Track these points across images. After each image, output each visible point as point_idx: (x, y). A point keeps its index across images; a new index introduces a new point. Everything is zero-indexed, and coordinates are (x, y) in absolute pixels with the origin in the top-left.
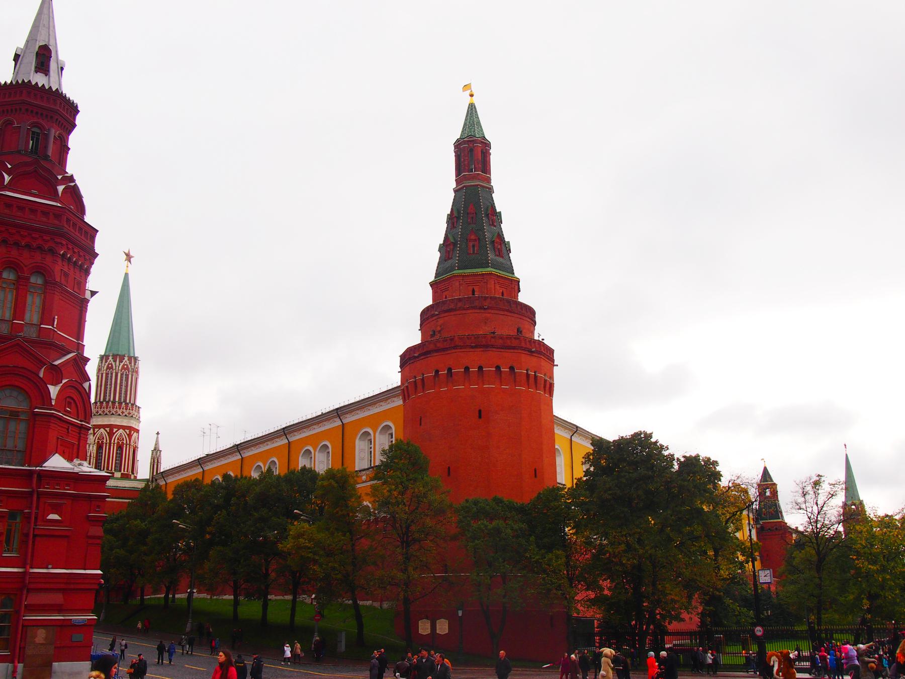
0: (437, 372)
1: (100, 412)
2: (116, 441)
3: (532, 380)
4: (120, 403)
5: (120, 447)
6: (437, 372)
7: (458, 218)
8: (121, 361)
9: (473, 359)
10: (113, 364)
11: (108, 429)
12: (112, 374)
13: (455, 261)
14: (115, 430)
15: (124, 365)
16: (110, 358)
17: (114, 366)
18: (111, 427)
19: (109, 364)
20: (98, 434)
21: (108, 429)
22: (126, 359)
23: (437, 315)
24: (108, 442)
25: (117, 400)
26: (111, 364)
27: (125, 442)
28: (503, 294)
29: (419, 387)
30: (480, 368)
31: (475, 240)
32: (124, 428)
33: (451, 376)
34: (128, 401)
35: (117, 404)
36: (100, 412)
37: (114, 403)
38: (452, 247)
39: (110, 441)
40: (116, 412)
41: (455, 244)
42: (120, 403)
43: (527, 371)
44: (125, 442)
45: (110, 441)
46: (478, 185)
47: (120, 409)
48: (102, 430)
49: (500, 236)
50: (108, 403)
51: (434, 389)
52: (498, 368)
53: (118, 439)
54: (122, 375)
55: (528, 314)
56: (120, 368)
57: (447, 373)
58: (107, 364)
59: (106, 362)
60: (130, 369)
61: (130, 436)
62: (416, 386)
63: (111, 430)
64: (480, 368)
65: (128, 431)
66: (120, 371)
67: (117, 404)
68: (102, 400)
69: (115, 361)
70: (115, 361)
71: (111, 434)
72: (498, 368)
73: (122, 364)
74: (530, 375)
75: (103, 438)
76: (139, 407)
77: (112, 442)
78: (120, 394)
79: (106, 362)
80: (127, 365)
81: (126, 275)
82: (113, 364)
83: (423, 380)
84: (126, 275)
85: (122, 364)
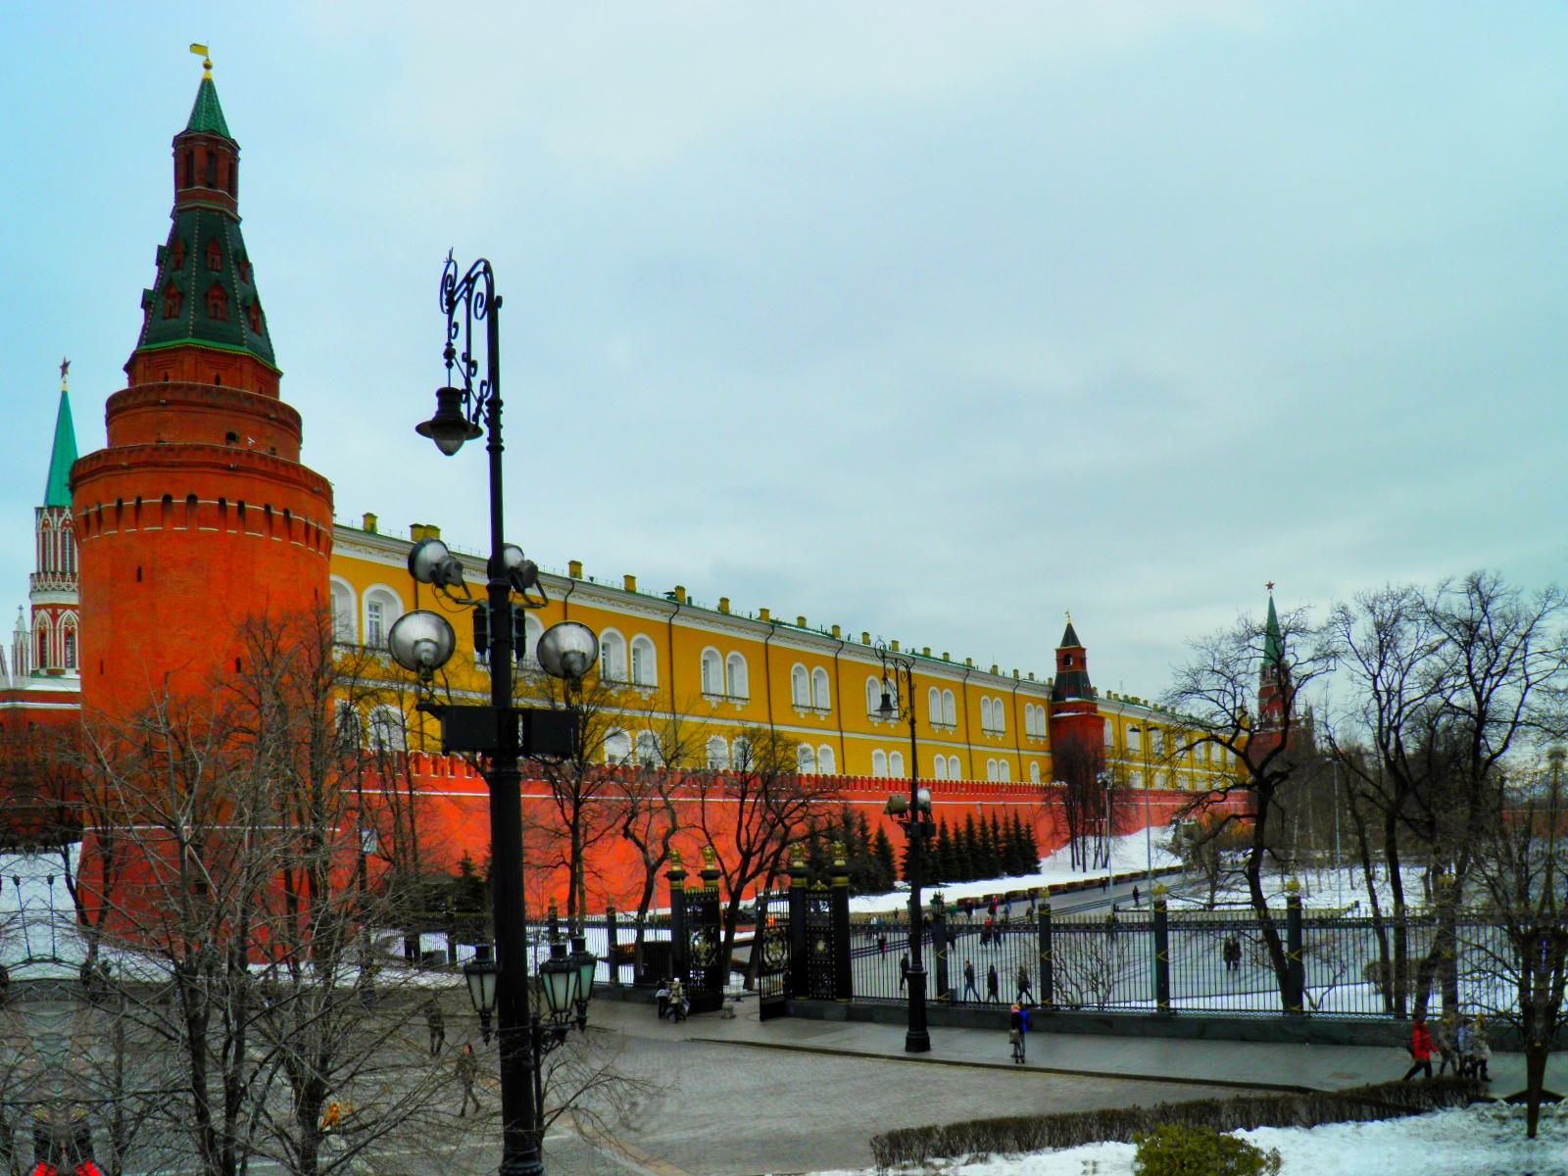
1: (39, 587)
4: (63, 574)
8: (60, 515)
9: (233, 488)
11: (50, 610)
14: (60, 611)
16: (46, 511)
18: (54, 607)
29: (93, 519)
36: (39, 587)
42: (63, 574)
45: (55, 626)
48: (43, 612)
50: (46, 573)
52: (222, 501)
54: (63, 534)
64: (192, 498)
69: (51, 515)
70: (51, 515)
71: (55, 617)
72: (222, 501)
73: (62, 519)
78: (64, 560)
84: (64, 395)
85: (62, 519)
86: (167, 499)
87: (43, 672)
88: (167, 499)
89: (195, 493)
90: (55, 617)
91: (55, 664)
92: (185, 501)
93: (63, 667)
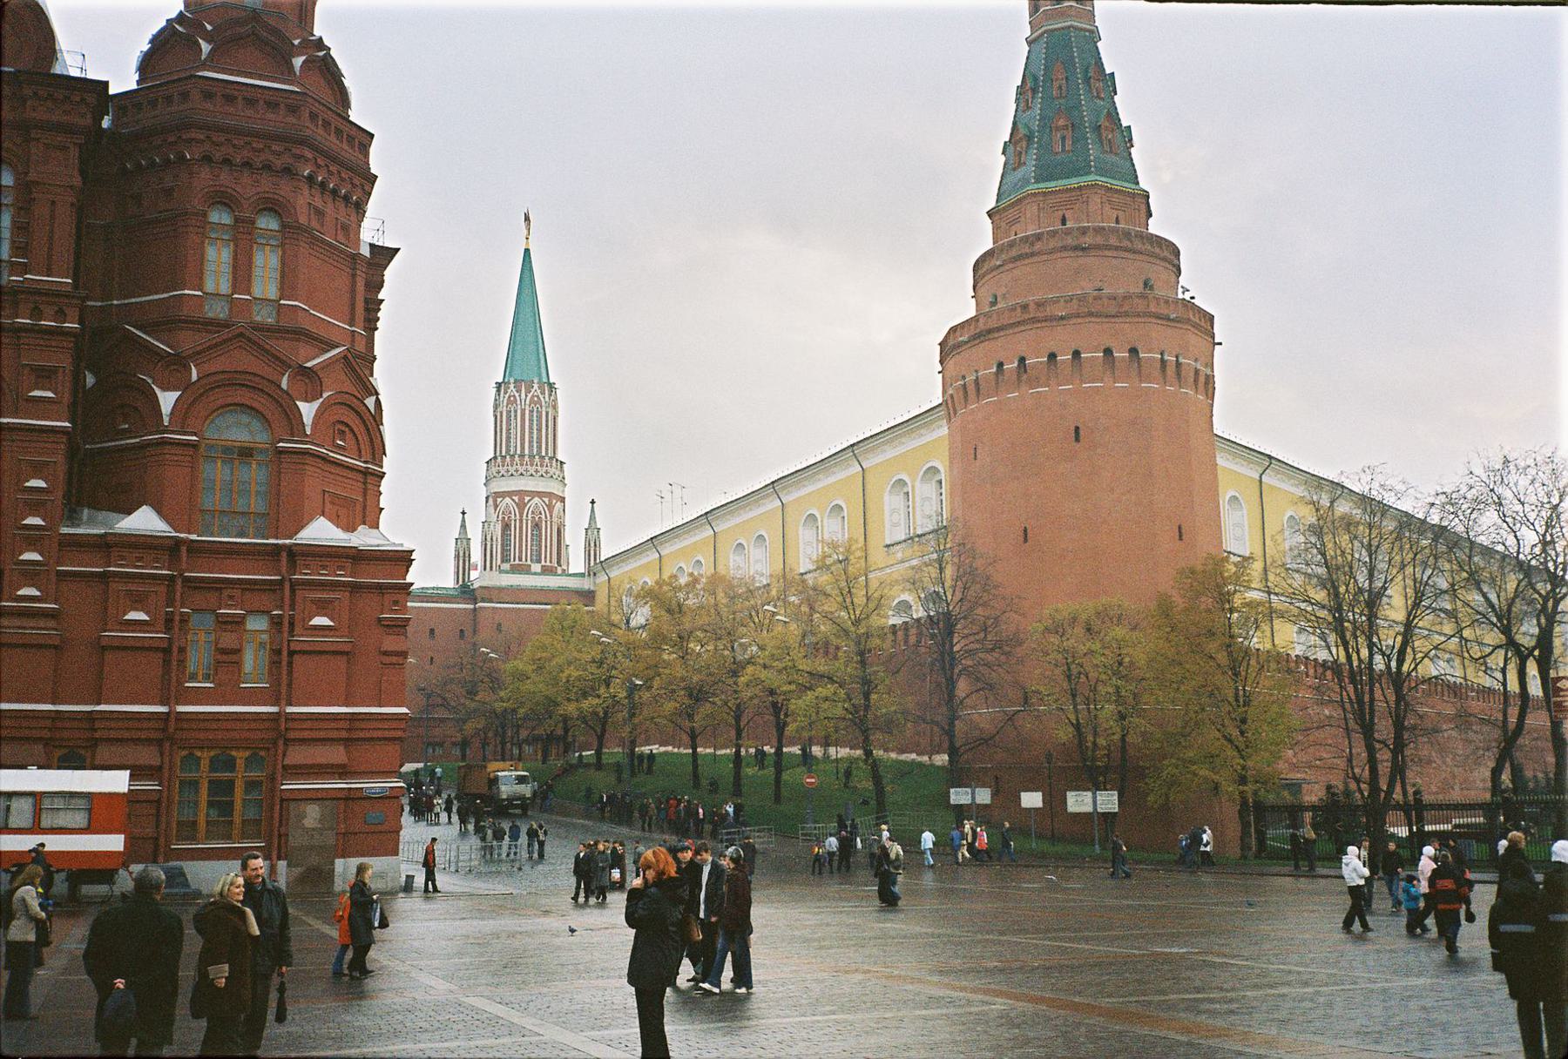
0: (1000, 365)
1: (502, 472)
2: (530, 516)
3: (1171, 370)
4: (532, 457)
5: (537, 526)
6: (1000, 365)
7: (1034, 91)
10: (517, 395)
11: (516, 498)
12: (516, 411)
13: (1029, 168)
14: (527, 499)
15: (533, 396)
17: (518, 398)
19: (509, 397)
20: (502, 506)
21: (516, 498)
22: (536, 386)
23: (1000, 266)
24: (518, 517)
25: (527, 452)
26: (514, 396)
27: (543, 517)
28: (1117, 221)
30: (1076, 354)
31: (1065, 127)
32: (540, 494)
33: (1026, 371)
34: (543, 454)
35: (527, 458)
37: (522, 456)
38: (1024, 144)
39: (521, 516)
40: (527, 471)
41: (1029, 138)
42: (532, 457)
43: (1162, 354)
44: (543, 517)
45: (521, 516)
46: (1069, 27)
47: (532, 465)
48: (508, 500)
49: (1113, 116)
51: (997, 395)
52: (1108, 352)
53: (533, 512)
54: (531, 411)
55: (1168, 254)
56: (528, 402)
57: (1019, 365)
58: (507, 396)
59: (505, 393)
60: (543, 404)
61: (550, 507)
62: (966, 392)
63: (522, 499)
64: (1076, 354)
65: (546, 500)
66: (527, 407)
67: (527, 458)
68: (504, 454)
69: (519, 391)
70: (519, 391)
71: (521, 506)
72: (1108, 352)
73: (530, 396)
74: (1168, 363)
75: (510, 513)
76: (561, 462)
77: (524, 517)
79: (505, 393)
80: (538, 396)
81: (527, 251)
82: (517, 395)
83: (977, 382)
84: (527, 251)
85: (530, 396)
86: (1052, 356)
87: (506, 566)
88: (1052, 356)
89: (1054, 350)
90: (521, 506)
91: (520, 560)
92: (1070, 357)
93: (529, 562)
